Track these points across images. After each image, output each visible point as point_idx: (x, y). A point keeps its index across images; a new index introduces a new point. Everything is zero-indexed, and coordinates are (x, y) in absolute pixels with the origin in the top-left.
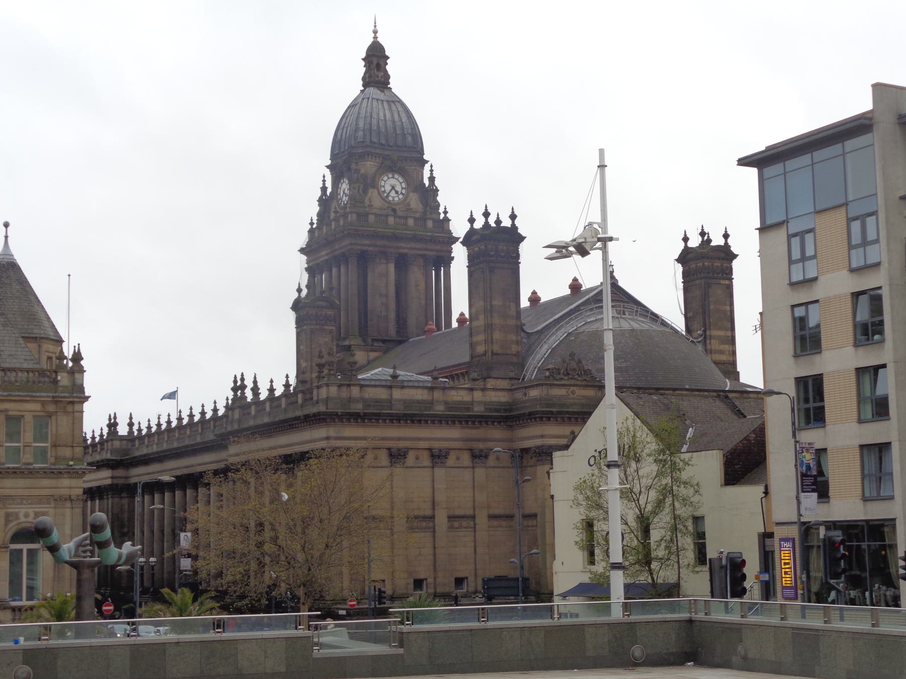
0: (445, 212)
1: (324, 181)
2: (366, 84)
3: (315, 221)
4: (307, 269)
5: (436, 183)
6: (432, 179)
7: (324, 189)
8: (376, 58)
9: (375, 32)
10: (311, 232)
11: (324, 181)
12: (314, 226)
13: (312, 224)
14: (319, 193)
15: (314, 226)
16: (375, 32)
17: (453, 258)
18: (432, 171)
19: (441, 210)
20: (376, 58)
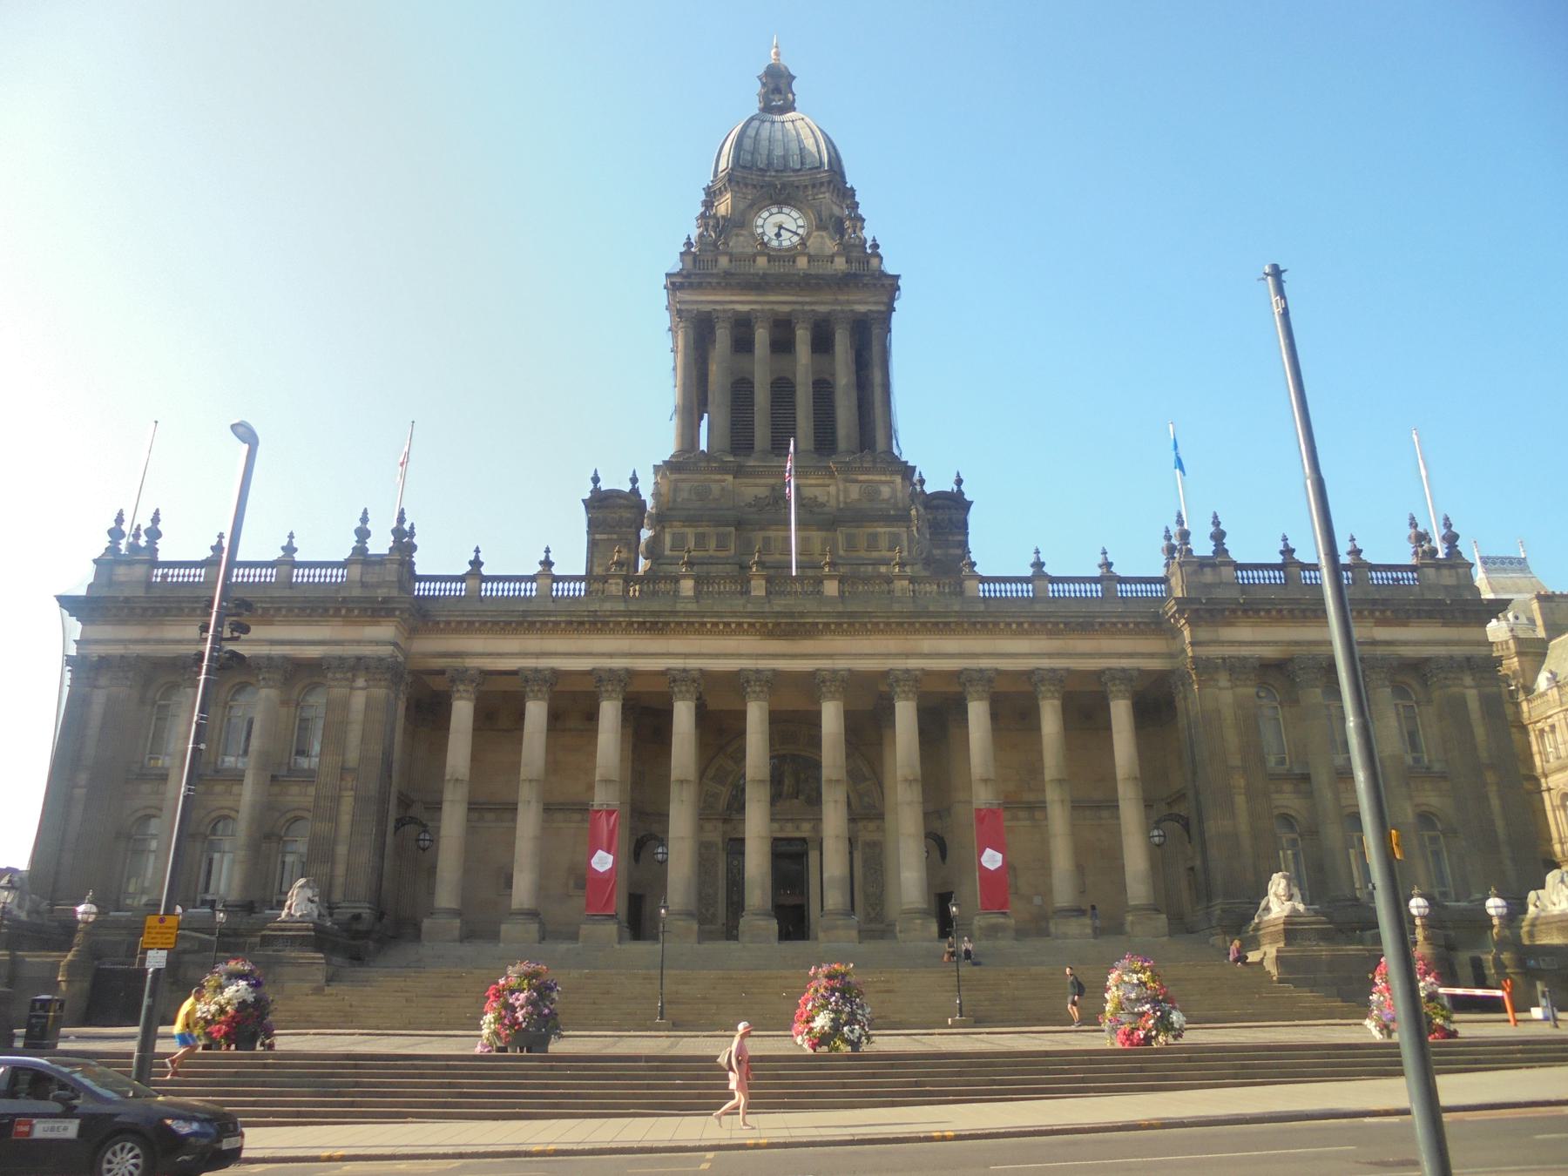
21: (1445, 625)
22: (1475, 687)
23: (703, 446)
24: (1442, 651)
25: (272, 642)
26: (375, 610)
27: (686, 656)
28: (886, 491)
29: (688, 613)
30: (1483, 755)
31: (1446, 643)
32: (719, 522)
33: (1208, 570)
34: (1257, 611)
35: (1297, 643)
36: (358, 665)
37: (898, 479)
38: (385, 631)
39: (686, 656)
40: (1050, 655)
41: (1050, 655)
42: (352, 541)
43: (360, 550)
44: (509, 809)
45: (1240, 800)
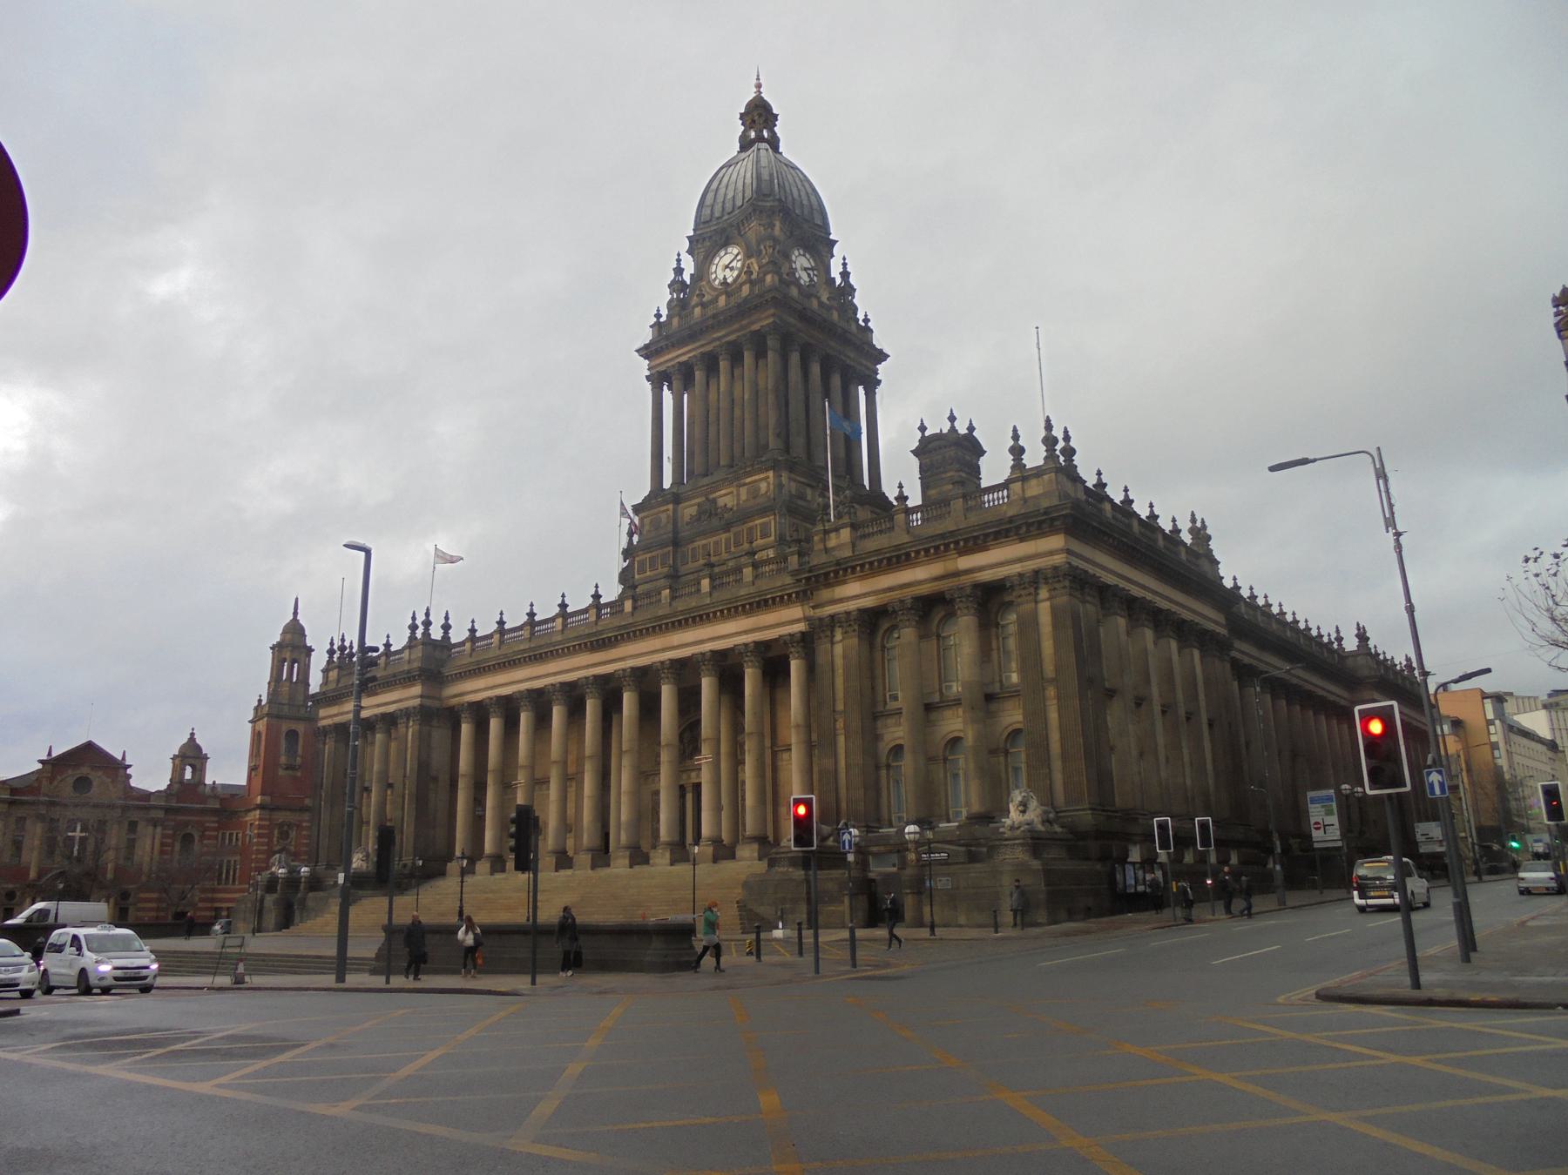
0: (866, 320)
1: (679, 261)
2: (745, 144)
3: (664, 312)
4: (648, 378)
5: (852, 280)
6: (845, 275)
7: (679, 271)
8: (759, 116)
9: (759, 86)
10: (658, 326)
11: (679, 261)
12: (663, 319)
13: (658, 316)
14: (672, 276)
15: (663, 319)
16: (759, 86)
17: (879, 382)
18: (845, 265)
19: (860, 316)
20: (759, 116)
21: (1022, 540)
22: (1049, 599)
23: (667, 484)
24: (1016, 568)
25: (379, 706)
26: (406, 679)
27: (555, 674)
28: (763, 486)
29: (560, 643)
30: (1049, 669)
31: (1020, 560)
32: (662, 545)
33: (833, 535)
34: (854, 568)
35: (890, 589)
36: (407, 713)
37: (771, 474)
38: (417, 690)
39: (555, 674)
40: (746, 632)
41: (746, 632)
42: (408, 633)
43: (412, 637)
44: (545, 781)
45: (841, 740)
